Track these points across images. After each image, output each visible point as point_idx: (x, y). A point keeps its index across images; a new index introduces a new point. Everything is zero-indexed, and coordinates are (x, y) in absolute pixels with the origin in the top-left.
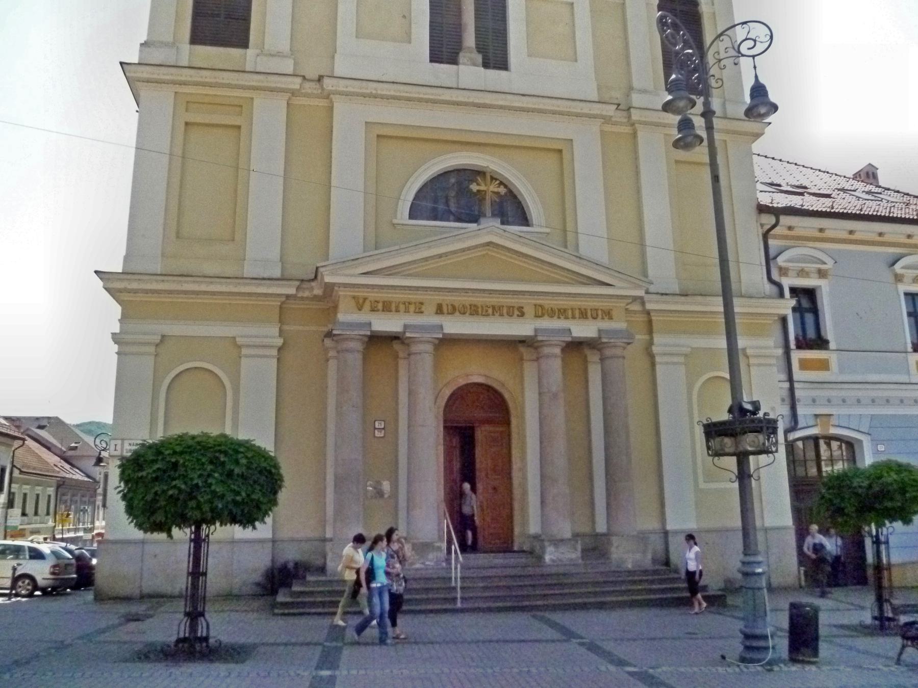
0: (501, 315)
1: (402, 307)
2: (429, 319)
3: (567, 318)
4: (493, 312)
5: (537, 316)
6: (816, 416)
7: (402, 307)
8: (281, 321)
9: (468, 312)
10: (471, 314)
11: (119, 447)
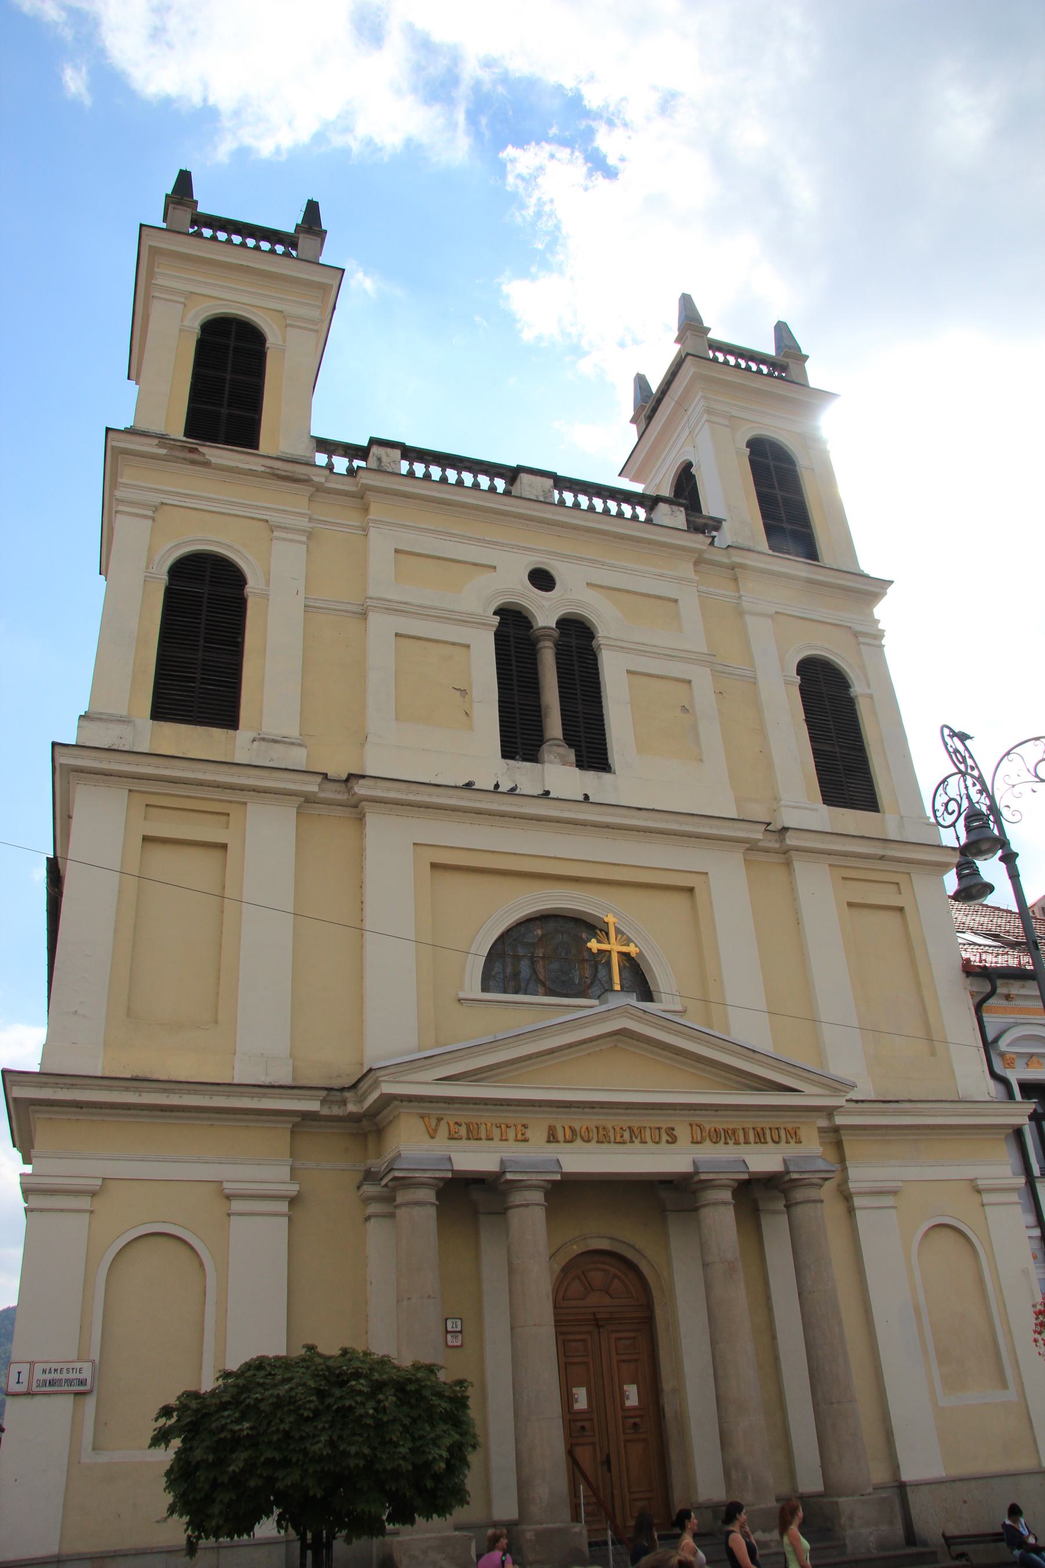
0: (644, 1142)
3: (737, 1143)
4: (631, 1137)
9: (595, 1139)
10: (598, 1142)
11: (24, 1378)
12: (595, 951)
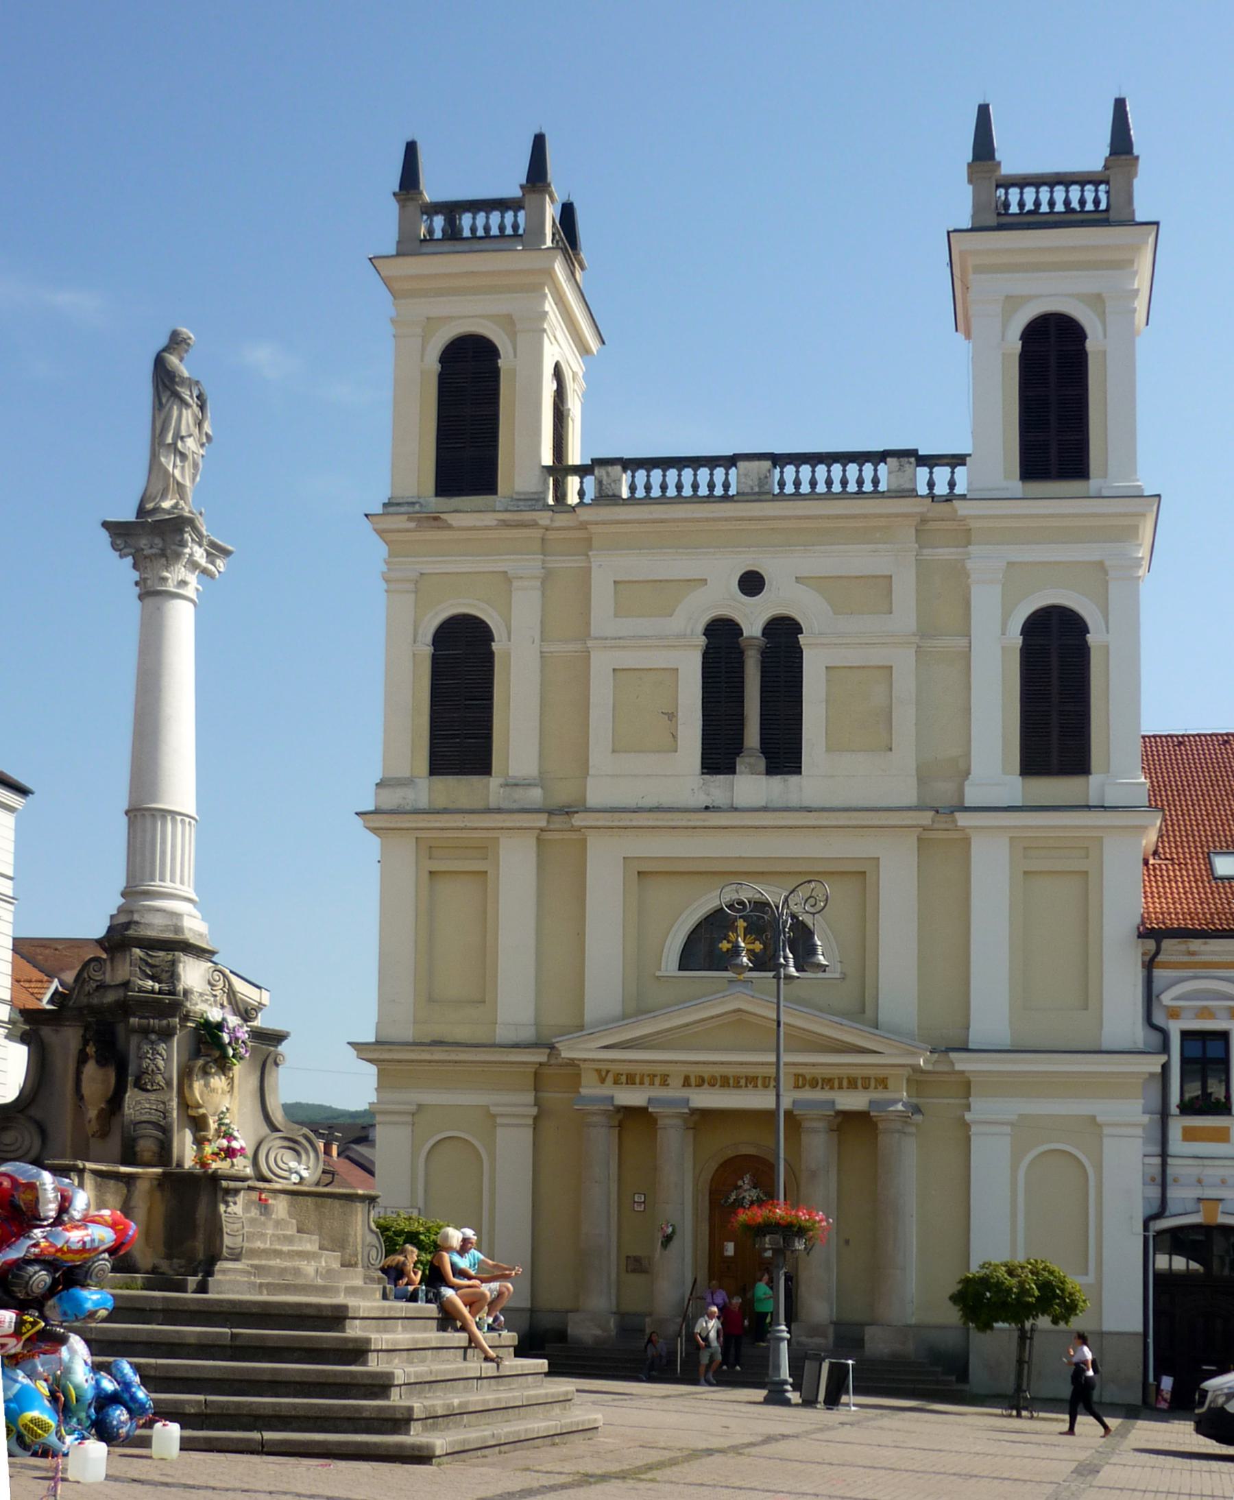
1: (647, 1080)
2: (674, 1092)
3: (832, 1088)
5: (797, 1087)
6: (1199, 1200)
7: (647, 1080)
8: (536, 1090)
9: (719, 1084)
12: (725, 950)
